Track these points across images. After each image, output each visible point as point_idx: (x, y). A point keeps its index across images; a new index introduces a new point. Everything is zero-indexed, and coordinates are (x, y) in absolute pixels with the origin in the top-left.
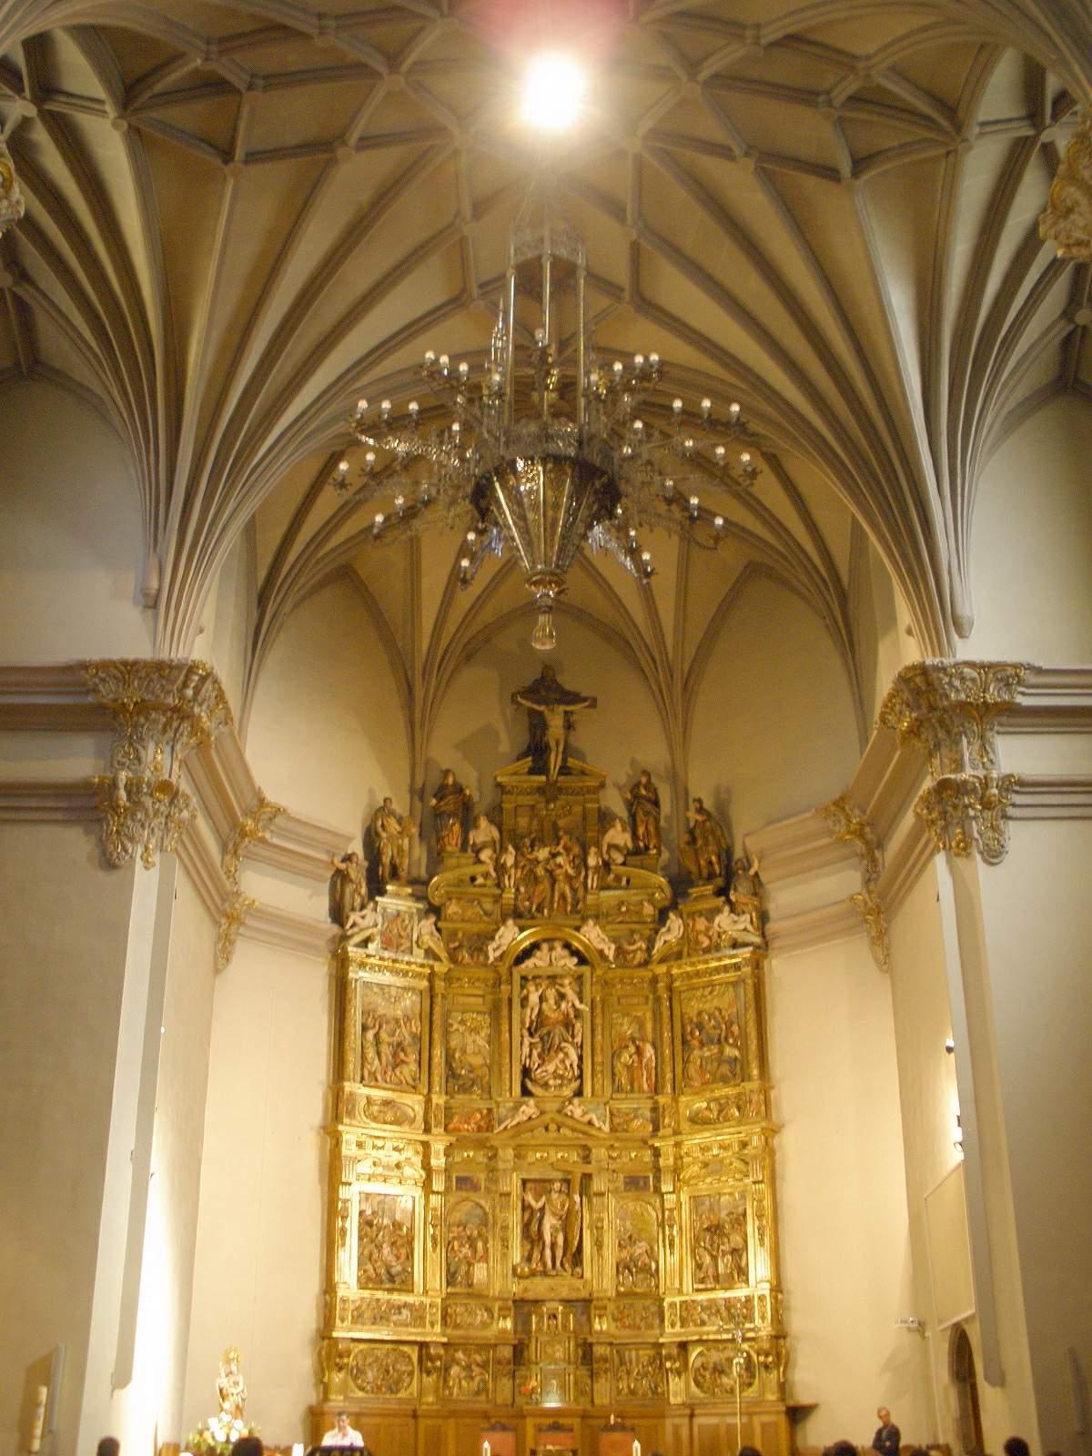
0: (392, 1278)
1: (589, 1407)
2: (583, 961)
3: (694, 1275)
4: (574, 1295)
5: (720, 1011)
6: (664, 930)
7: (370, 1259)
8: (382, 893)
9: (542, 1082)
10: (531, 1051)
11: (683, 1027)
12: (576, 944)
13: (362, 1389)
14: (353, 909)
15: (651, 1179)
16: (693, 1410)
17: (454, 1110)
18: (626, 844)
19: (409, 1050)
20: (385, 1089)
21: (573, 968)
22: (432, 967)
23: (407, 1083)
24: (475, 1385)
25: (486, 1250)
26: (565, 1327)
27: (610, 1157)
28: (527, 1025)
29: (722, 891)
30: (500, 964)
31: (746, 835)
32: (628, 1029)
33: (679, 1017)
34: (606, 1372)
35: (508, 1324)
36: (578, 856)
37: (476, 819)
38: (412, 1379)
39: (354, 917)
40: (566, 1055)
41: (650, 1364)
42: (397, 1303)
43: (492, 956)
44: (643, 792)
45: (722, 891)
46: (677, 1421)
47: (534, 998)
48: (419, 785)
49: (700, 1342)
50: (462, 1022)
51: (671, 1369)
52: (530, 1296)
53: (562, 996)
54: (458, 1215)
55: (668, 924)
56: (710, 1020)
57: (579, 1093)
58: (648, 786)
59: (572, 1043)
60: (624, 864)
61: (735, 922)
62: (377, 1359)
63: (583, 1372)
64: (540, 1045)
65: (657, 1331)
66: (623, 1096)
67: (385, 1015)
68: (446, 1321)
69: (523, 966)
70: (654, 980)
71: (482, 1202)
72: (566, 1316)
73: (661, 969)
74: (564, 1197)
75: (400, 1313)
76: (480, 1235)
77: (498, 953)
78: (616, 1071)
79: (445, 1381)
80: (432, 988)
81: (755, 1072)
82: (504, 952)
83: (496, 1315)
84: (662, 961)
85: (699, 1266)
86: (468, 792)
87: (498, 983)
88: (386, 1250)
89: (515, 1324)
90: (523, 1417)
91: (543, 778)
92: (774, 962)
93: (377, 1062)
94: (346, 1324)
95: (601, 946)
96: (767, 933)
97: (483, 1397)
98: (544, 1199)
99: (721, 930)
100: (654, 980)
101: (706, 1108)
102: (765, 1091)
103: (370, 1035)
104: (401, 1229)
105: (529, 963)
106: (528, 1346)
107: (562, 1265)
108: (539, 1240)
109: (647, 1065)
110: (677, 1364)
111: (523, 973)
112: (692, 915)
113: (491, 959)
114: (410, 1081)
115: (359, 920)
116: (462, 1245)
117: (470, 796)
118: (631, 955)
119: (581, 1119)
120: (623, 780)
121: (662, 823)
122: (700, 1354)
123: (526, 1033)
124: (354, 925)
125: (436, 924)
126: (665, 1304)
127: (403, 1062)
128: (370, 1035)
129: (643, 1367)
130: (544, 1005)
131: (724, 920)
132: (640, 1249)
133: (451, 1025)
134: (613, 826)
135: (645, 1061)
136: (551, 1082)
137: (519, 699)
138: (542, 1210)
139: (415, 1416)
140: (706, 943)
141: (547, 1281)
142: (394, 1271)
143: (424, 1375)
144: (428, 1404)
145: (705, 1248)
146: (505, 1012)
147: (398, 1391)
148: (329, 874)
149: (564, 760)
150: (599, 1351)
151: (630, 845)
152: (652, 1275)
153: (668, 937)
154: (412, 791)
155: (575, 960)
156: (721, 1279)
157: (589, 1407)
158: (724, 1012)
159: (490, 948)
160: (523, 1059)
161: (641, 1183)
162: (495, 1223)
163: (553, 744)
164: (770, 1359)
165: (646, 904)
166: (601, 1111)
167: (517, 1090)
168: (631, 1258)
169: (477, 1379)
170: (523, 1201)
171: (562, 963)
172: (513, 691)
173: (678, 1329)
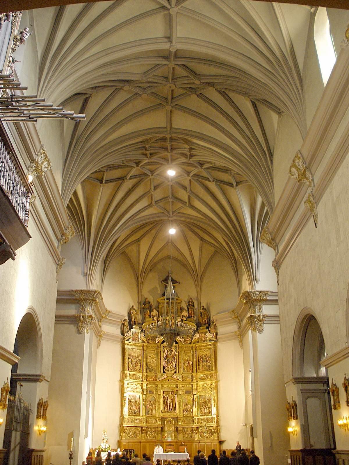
1: (177, 441)
4: (174, 417)
5: (207, 355)
8: (132, 328)
13: (129, 437)
14: (126, 332)
16: (199, 441)
19: (138, 363)
22: (143, 344)
24: (153, 436)
25: (155, 406)
29: (208, 328)
31: (213, 316)
35: (160, 423)
37: (153, 310)
39: (126, 334)
40: (173, 364)
44: (191, 303)
45: (208, 328)
47: (166, 351)
48: (140, 301)
50: (150, 356)
52: (165, 417)
57: (175, 372)
58: (192, 302)
60: (186, 320)
63: (176, 433)
65: (192, 424)
70: (192, 347)
71: (154, 396)
73: (194, 345)
77: (158, 341)
79: (146, 435)
80: (143, 349)
81: (214, 369)
84: (194, 343)
85: (201, 411)
87: (158, 347)
88: (134, 407)
89: (161, 423)
90: (163, 443)
96: (217, 338)
97: (155, 439)
100: (192, 347)
103: (130, 360)
107: (172, 410)
111: (164, 346)
112: (201, 333)
115: (127, 335)
120: (186, 300)
121: (195, 310)
122: (201, 429)
123: (164, 359)
124: (126, 336)
128: (130, 360)
131: (208, 334)
132: (189, 406)
136: (170, 370)
138: (167, 398)
140: (204, 339)
142: (135, 411)
144: (143, 440)
147: (136, 437)
150: (179, 429)
151: (187, 315)
154: (138, 302)
157: (177, 441)
164: (216, 431)
167: (162, 372)
172: (162, 280)
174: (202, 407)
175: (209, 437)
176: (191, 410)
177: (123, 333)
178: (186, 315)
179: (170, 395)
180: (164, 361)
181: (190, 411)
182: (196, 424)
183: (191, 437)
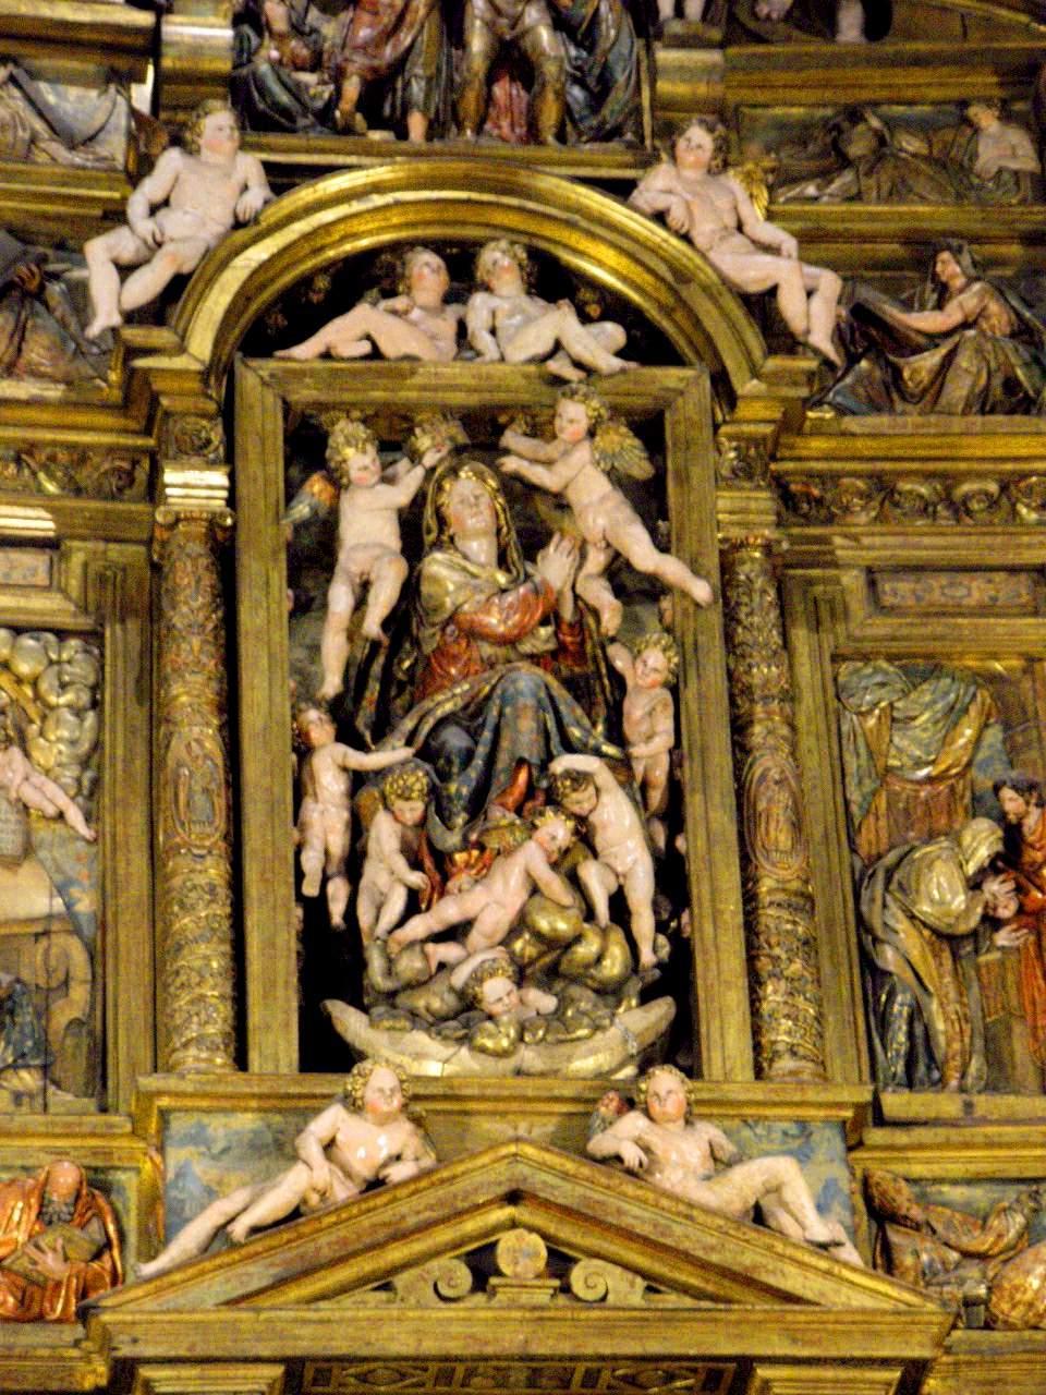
2: (647, 345)
9: (436, 1000)
10: (357, 828)
12: (602, 265)
21: (608, 362)
28: (332, 684)
30: (161, 336)
40: (585, 836)
43: (109, 301)
59: (622, 766)
64: (419, 780)
66: (948, 1105)
69: (306, 351)
77: (146, 285)
78: (889, 958)
95: (753, 272)
105: (343, 334)
111: (303, 394)
113: (105, 315)
118: (929, 361)
123: (319, 727)
136: (497, 990)
146: (191, 603)
155: (614, 333)
160: (312, 862)
165: (987, 119)
171: (536, 340)
180: (329, 781)
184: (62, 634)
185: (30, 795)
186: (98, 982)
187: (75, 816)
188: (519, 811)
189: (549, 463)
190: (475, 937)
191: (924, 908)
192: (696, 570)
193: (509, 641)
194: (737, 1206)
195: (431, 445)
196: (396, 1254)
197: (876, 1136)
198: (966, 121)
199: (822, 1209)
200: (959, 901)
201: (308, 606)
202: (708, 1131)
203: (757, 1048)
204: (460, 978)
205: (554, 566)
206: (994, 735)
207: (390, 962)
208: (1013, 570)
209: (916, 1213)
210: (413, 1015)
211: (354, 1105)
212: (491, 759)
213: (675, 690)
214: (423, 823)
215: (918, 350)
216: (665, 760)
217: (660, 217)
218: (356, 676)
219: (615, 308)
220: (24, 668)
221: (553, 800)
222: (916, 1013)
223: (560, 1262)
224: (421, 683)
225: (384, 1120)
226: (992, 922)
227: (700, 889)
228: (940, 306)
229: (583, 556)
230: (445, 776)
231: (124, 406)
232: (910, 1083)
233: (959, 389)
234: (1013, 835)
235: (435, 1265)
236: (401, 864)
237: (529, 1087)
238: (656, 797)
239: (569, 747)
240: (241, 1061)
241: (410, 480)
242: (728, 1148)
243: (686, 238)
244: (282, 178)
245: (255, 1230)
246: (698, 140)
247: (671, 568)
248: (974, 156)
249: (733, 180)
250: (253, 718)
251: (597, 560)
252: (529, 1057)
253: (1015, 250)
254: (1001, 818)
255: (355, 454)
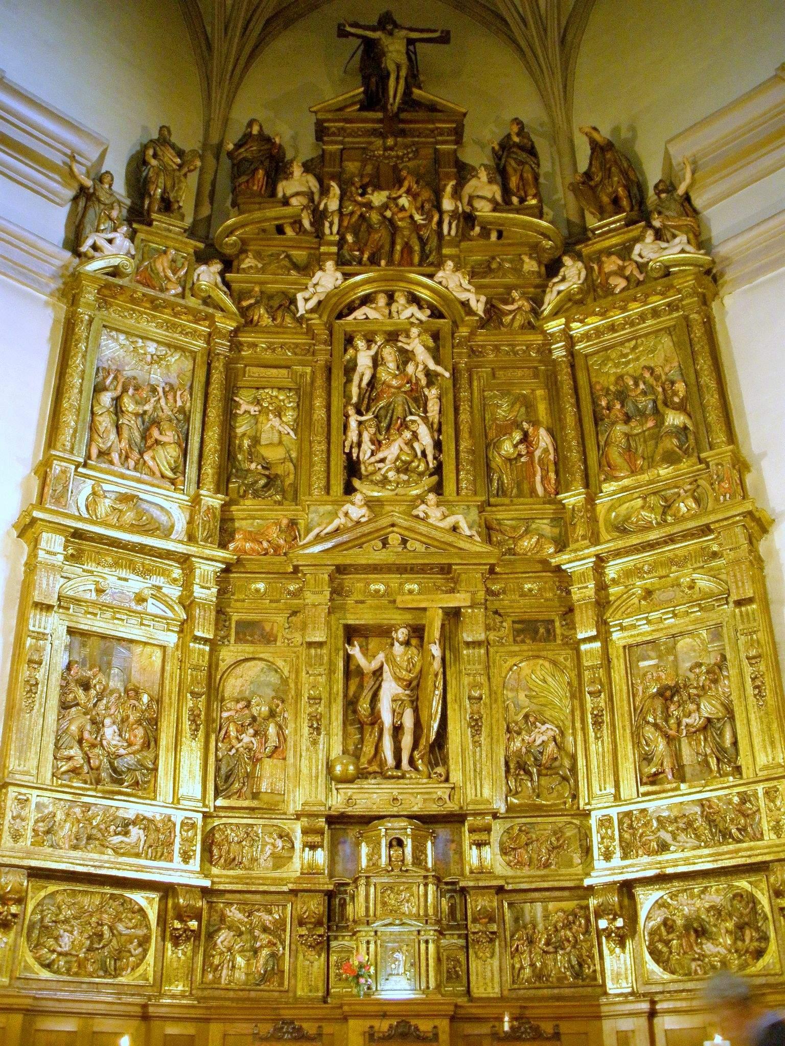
0: (117, 776)
3: (639, 771)
4: (434, 809)
5: (651, 370)
6: (556, 280)
7: (80, 742)
9: (378, 477)
10: (360, 435)
11: (595, 403)
12: (424, 294)
13: (48, 966)
15: (557, 624)
16: (653, 1003)
17: (237, 524)
18: (494, 197)
20: (123, 477)
23: (163, 476)
26: (418, 860)
27: (489, 592)
28: (355, 399)
32: (503, 410)
33: (588, 391)
34: (491, 941)
35: (320, 857)
36: (428, 201)
38: (145, 951)
40: (415, 436)
41: (568, 926)
42: (121, 813)
44: (516, 139)
46: (625, 1024)
48: (215, 140)
49: (662, 879)
51: (608, 933)
53: (406, 357)
54: (239, 682)
55: (561, 273)
56: (636, 384)
57: (438, 489)
59: (425, 419)
61: (665, 249)
62: (82, 911)
66: (506, 501)
67: (135, 378)
68: (211, 852)
71: (280, 663)
72: (419, 851)
73: (555, 326)
74: (413, 651)
75: (126, 833)
76: (272, 714)
77: (312, 304)
78: (493, 465)
82: (320, 302)
83: (298, 845)
84: (555, 314)
85: (647, 758)
86: (277, 140)
88: (110, 732)
90: (345, 1019)
91: (380, 115)
92: (728, 300)
93: (113, 436)
94: (21, 844)
95: (463, 296)
97: (274, 986)
98: (381, 657)
99: (645, 260)
101: (643, 507)
102: (741, 465)
103: (106, 398)
104: (137, 697)
105: (359, 314)
106: (353, 898)
107: (412, 762)
108: (373, 724)
109: (540, 460)
110: (620, 922)
111: (348, 329)
113: (301, 311)
114: (169, 474)
115: (101, 243)
116: (242, 729)
117: (280, 145)
118: (511, 317)
119: (441, 524)
122: (660, 904)
123: (351, 411)
125: (222, 274)
126: (593, 822)
127: (157, 442)
128: (106, 398)
129: (556, 930)
130: (380, 369)
132: (542, 734)
133: (238, 405)
134: (476, 176)
135: (537, 454)
136: (391, 475)
137: (348, 29)
138: (378, 673)
139: (145, 1017)
140: (622, 283)
141: (388, 785)
143: (169, 945)
144: (173, 996)
145: (656, 726)
147: (117, 973)
148: (70, 193)
149: (407, 93)
151: (499, 198)
152: (565, 779)
153: (562, 287)
156: (688, 771)
157: (461, 1001)
158: (658, 371)
159: (300, 297)
160: (347, 444)
161: (542, 630)
162: (298, 695)
163: (391, 67)
165: (526, 259)
166: (474, 514)
167: (338, 487)
168: (528, 751)
169: (265, 952)
170: (348, 658)
171: (407, 313)
173: (616, 861)
174: (649, 732)
175: (735, 961)
176: (567, 763)
177: (73, 243)
178: (489, 196)
179: (398, 649)
180: (353, 424)
181: (548, 769)
182: (616, 861)
183: (578, 975)
184: (290, 390)
185: (281, 429)
186: (296, 474)
187: (292, 434)
188: (398, 430)
189: (408, 344)
190: (387, 461)
191: (503, 452)
192: (446, 370)
193: (399, 388)
194: (448, 527)
195: (379, 340)
196: (363, 540)
197: (489, 508)
198: (521, 259)
199: (470, 528)
200: (512, 450)
201: (349, 381)
202: (443, 509)
203: (458, 488)
204: (383, 472)
205: (410, 368)
206: (523, 410)
207: (366, 468)
208: (529, 368)
209: (497, 527)
210: (372, 481)
211: (353, 504)
212: (391, 418)
213: (440, 399)
214: (375, 434)
215: (507, 315)
216: (437, 416)
217: (440, 283)
218: (361, 397)
219: (431, 306)
220: (281, 398)
221: (407, 428)
222: (500, 479)
223: (404, 541)
224: (377, 399)
225: (361, 507)
226: (520, 455)
227: (445, 448)
228: (512, 304)
229: (417, 366)
230: (380, 422)
231: (307, 333)
232: (498, 495)
233: (517, 324)
234: (526, 435)
235: (373, 542)
236: (369, 444)
237: (399, 498)
238: (435, 426)
239: (411, 414)
240: (328, 493)
241: (374, 348)
242: (447, 513)
243: (447, 288)
244: (347, 276)
245: (327, 534)
246: (450, 264)
247: (439, 369)
248: (522, 267)
249: (457, 274)
250: (334, 409)
251: (421, 367)
252: (400, 491)
253: (532, 290)
254: (522, 429)
255: (360, 344)
